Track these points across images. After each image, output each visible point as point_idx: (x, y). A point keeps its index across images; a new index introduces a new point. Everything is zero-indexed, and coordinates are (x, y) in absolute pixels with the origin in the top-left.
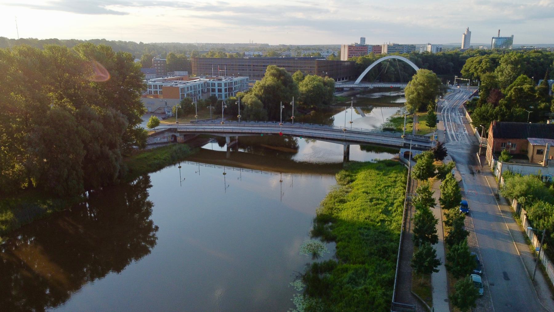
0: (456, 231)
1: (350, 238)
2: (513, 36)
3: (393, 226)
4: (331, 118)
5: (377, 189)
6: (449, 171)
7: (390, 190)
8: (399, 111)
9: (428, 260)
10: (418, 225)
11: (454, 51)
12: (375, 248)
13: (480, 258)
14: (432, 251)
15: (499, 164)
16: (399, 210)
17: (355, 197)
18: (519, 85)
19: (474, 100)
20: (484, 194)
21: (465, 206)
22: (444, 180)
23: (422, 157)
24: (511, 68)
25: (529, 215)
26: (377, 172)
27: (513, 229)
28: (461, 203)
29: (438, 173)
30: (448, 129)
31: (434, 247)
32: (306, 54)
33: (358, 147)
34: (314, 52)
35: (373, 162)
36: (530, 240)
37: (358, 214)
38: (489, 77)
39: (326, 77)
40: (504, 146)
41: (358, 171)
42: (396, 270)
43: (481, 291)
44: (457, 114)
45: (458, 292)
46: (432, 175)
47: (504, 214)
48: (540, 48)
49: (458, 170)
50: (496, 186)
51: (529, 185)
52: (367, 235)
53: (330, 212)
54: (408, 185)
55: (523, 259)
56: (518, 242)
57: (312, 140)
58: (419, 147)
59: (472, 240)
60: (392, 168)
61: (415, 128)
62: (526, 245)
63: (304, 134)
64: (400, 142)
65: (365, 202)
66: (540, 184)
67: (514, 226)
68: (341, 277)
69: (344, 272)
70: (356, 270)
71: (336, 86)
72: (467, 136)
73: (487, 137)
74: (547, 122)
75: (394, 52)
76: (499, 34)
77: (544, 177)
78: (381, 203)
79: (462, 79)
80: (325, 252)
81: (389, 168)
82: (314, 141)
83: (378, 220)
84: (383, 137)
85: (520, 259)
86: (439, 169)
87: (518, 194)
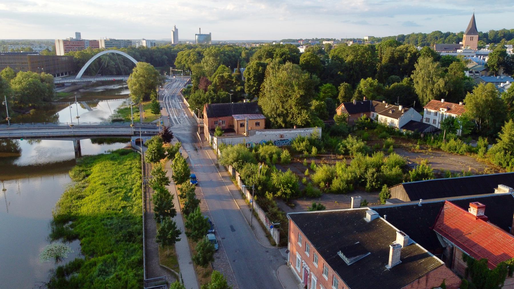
0: (190, 201)
1: (94, 232)
2: (210, 33)
3: (135, 210)
4: (55, 115)
5: (114, 178)
6: (177, 150)
7: (127, 177)
8: (125, 102)
9: (170, 232)
10: (157, 204)
11: (166, 46)
12: (121, 235)
13: (212, 220)
14: (173, 223)
15: (215, 139)
16: (139, 193)
17: (93, 191)
18: (220, 73)
19: (189, 87)
20: (208, 165)
21: (194, 178)
22: (174, 159)
23: (152, 142)
24: (213, 59)
25: (242, 175)
26: (112, 162)
27: (232, 189)
28: (190, 177)
29: (168, 154)
30: (171, 115)
31: (174, 219)
32: (14, 49)
33: (88, 141)
34: (25, 47)
35: (106, 153)
36: (245, 196)
37: (98, 207)
38: (197, 67)
39: (43, 73)
40: (217, 124)
41: (92, 164)
42: (143, 249)
43: (216, 246)
44: (176, 101)
45: (199, 253)
46: (163, 157)
47: (224, 179)
48: (231, 43)
49: (184, 149)
50: (215, 157)
51: (238, 152)
52: (110, 224)
53: (69, 211)
54: (143, 168)
55: (242, 211)
56: (237, 199)
57: (36, 140)
58: (148, 133)
59: (204, 207)
60: (126, 156)
61: (141, 116)
62: (243, 200)
63: (25, 135)
64: (130, 131)
65: (104, 193)
66: (246, 150)
67: (232, 187)
68: (91, 272)
69: (92, 267)
70: (105, 261)
71: (56, 82)
72: (187, 119)
73: (203, 118)
74: (243, 101)
75: (111, 46)
76: (200, 32)
77: (248, 145)
78: (120, 191)
79: (176, 70)
80: (69, 252)
81: (123, 157)
82: (39, 142)
83: (119, 208)
84: (113, 128)
85: (240, 212)
86: (168, 150)
87: (232, 161)
